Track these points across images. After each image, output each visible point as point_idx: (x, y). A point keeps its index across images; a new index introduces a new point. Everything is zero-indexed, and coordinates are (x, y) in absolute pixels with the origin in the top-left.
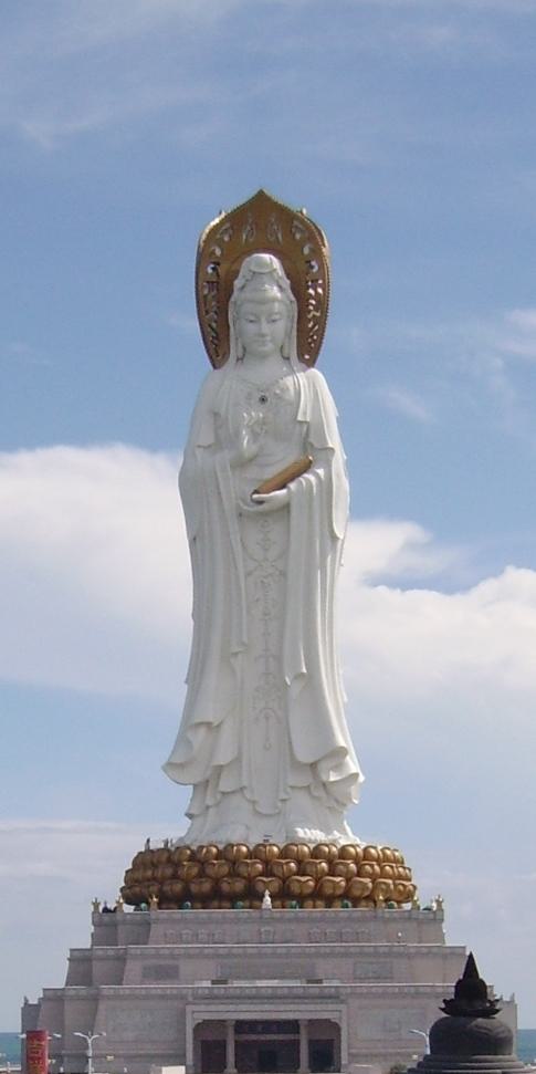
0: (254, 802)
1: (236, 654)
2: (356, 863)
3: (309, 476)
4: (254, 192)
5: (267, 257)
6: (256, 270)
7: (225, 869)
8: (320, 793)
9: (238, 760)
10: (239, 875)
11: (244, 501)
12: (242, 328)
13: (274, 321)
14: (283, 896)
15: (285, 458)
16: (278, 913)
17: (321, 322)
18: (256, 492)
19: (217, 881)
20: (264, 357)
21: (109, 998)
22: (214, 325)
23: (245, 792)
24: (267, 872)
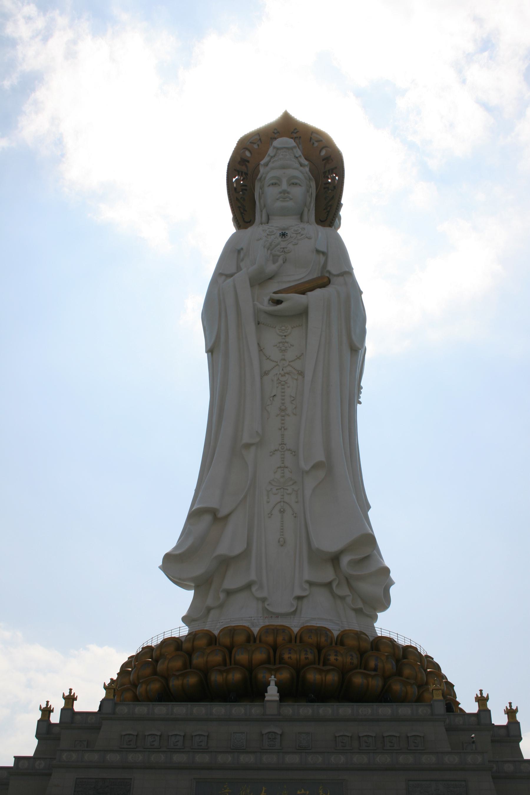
1: (248, 446)
7: (217, 658)
8: (344, 591)
9: (246, 554)
16: (289, 709)
18: (275, 293)
23: (254, 589)
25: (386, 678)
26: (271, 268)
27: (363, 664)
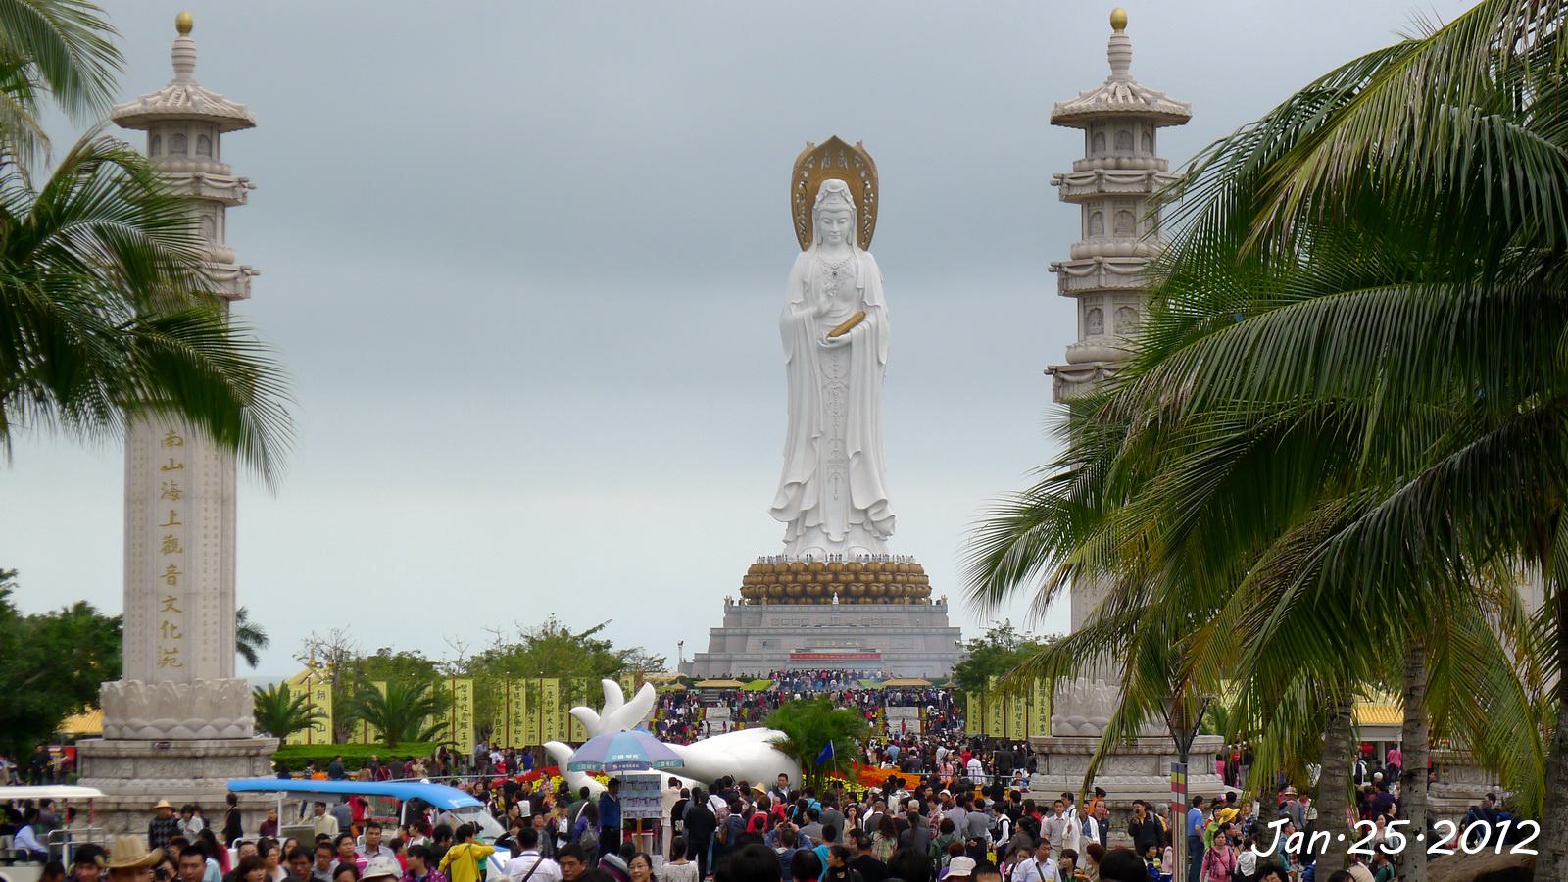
0: (828, 534)
2: (892, 573)
3: (864, 325)
4: (829, 137)
5: (836, 182)
6: (832, 191)
8: (870, 528)
9: (817, 507)
10: (818, 582)
11: (822, 341)
12: (820, 226)
13: (842, 223)
14: (848, 596)
15: (847, 311)
16: (842, 608)
17: (873, 222)
18: (830, 335)
19: (804, 584)
20: (834, 245)
21: (737, 660)
22: (803, 222)
24: (836, 580)
25: (886, 584)
26: (826, 306)
27: (877, 581)
